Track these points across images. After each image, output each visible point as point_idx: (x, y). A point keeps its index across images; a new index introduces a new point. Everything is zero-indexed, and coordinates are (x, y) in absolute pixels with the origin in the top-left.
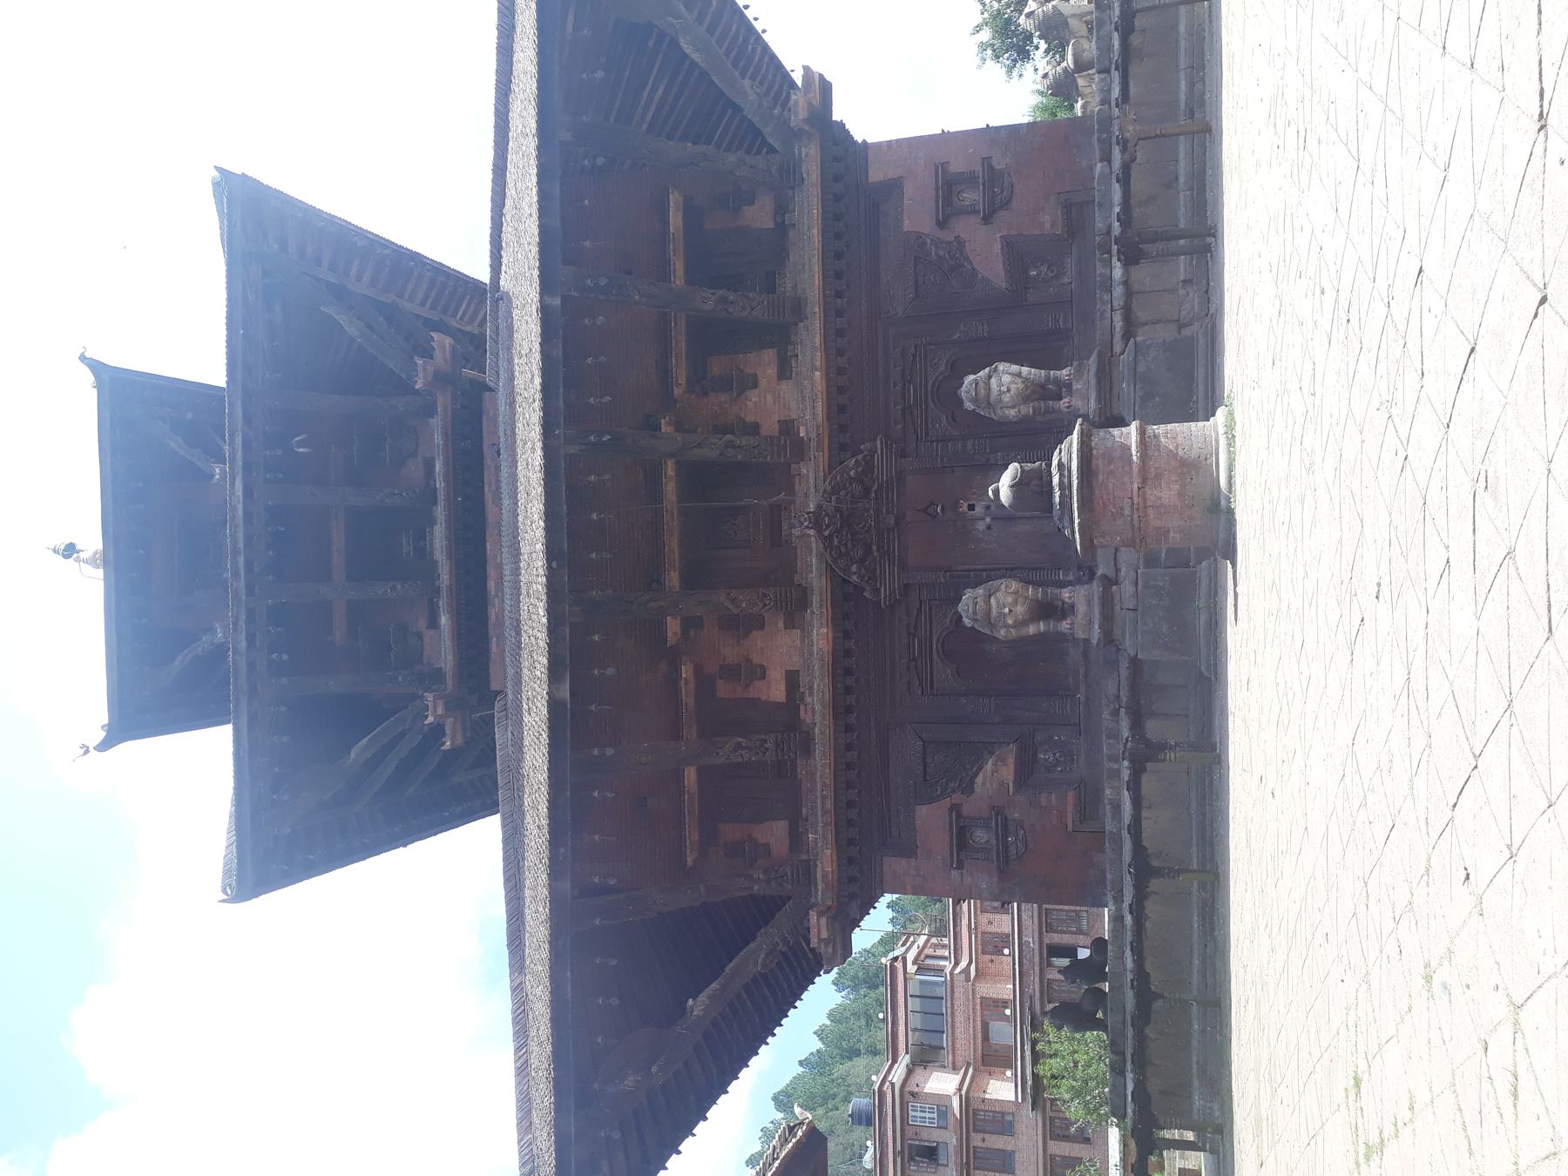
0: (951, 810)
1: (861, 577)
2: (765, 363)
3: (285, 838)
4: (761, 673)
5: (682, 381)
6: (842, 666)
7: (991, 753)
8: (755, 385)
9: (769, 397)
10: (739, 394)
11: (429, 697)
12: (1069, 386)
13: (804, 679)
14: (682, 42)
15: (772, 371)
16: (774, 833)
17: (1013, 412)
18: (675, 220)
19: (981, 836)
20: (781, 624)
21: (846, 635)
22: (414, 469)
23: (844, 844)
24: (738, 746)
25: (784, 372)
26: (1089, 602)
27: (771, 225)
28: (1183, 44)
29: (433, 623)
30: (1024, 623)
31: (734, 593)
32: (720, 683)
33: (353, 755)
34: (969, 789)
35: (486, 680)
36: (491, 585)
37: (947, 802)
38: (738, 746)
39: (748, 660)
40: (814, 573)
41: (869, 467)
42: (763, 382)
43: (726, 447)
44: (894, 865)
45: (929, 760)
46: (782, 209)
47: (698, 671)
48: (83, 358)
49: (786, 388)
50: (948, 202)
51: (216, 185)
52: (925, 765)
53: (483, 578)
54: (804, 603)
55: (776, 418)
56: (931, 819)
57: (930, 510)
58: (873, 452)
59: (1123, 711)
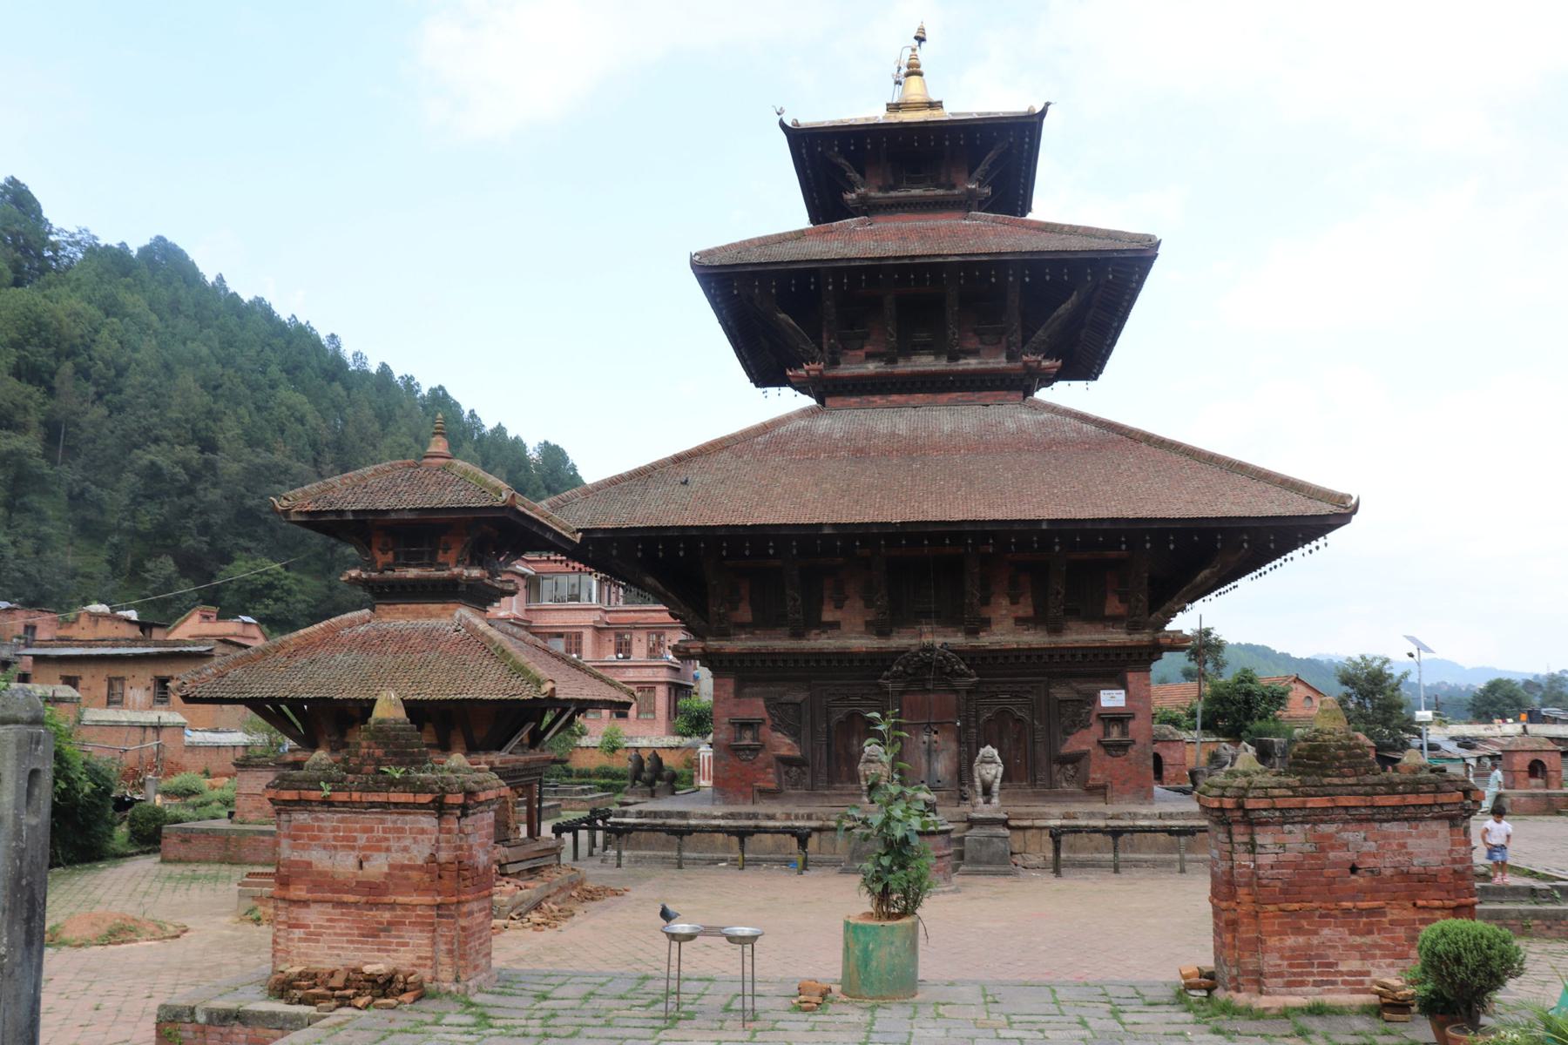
2: (1026, 609)
4: (839, 606)
6: (844, 659)
12: (988, 802)
13: (837, 632)
14: (1206, 572)
15: (1021, 613)
16: (745, 614)
18: (1113, 554)
19: (747, 739)
21: (862, 661)
22: (972, 342)
23: (741, 657)
24: (795, 600)
25: (1020, 621)
27: (1108, 612)
28: (1168, 856)
29: (870, 357)
33: (782, 316)
34: (774, 729)
35: (832, 394)
36: (894, 397)
37: (766, 716)
38: (795, 600)
40: (899, 641)
41: (962, 675)
42: (1014, 608)
44: (730, 685)
46: (1115, 620)
48: (1048, 104)
49: (1010, 622)
50: (1112, 720)
51: (1150, 238)
53: (900, 392)
54: (883, 633)
56: (756, 708)
58: (970, 676)
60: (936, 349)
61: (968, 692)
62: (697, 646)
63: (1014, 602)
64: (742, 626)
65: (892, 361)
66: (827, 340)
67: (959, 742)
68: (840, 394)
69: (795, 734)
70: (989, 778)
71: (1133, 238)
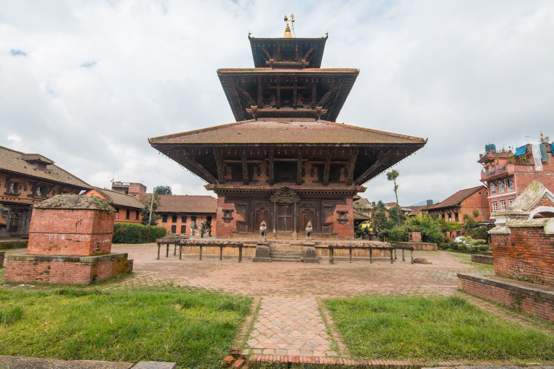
3: (230, 80)
11: (256, 107)
16: (229, 177)
19: (228, 216)
22: (301, 103)
25: (313, 182)
35: (259, 117)
46: (342, 182)
51: (356, 70)
54: (272, 184)
56: (231, 206)
60: (291, 106)
62: (213, 186)
63: (312, 176)
64: (228, 181)
65: (278, 108)
66: (260, 100)
68: (262, 117)
71: (352, 70)
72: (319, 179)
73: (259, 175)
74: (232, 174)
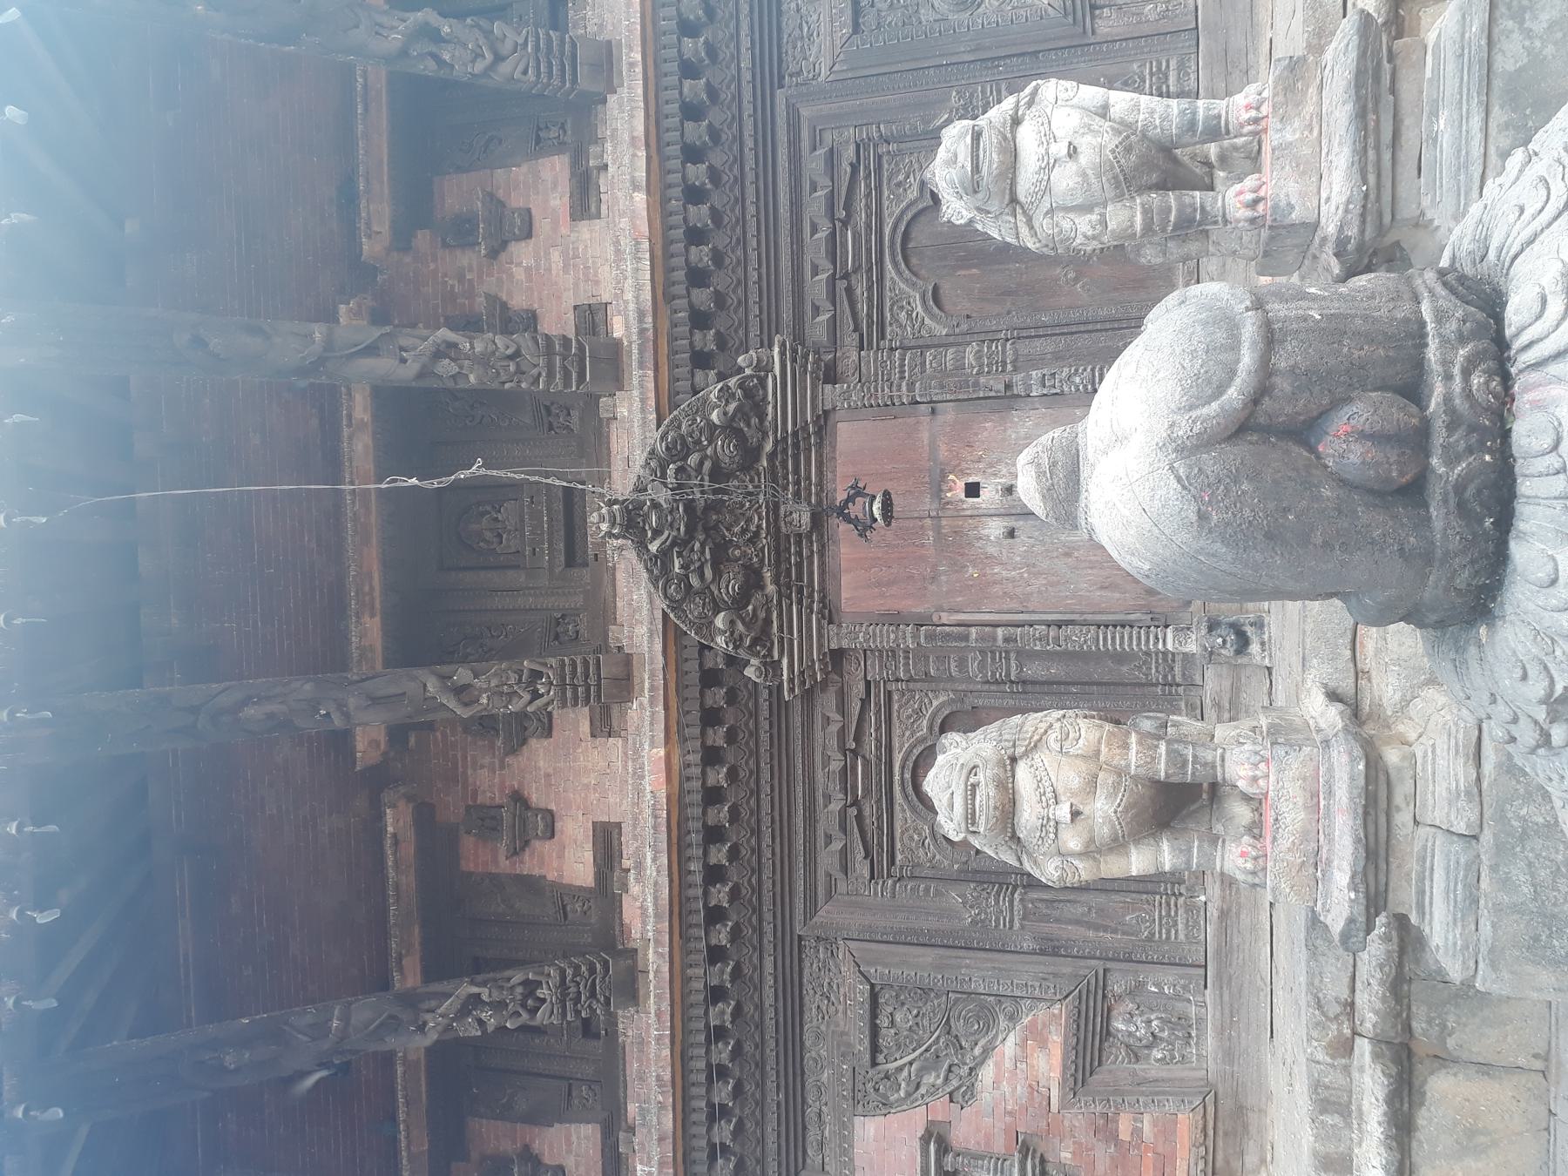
0: (925, 1140)
1: (737, 642)
2: (544, 184)
5: (383, 227)
7: (1013, 1018)
8: (528, 234)
9: (556, 256)
10: (494, 254)
17: (1084, 224)
20: (585, 727)
21: (711, 757)
26: (1315, 800)
30: (1118, 845)
31: (462, 675)
32: (468, 843)
34: (963, 1094)
39: (519, 799)
42: (542, 225)
43: (438, 355)
45: (883, 1021)
47: (425, 817)
52: (875, 1031)
54: (624, 685)
55: (569, 300)
57: (855, 510)
58: (763, 368)
59: (1364, 1047)
61: (831, 375)
67: (1009, 399)
69: (987, 1013)
70: (1097, 144)
72: (560, 147)
73: (529, 822)
74: (541, 1117)
